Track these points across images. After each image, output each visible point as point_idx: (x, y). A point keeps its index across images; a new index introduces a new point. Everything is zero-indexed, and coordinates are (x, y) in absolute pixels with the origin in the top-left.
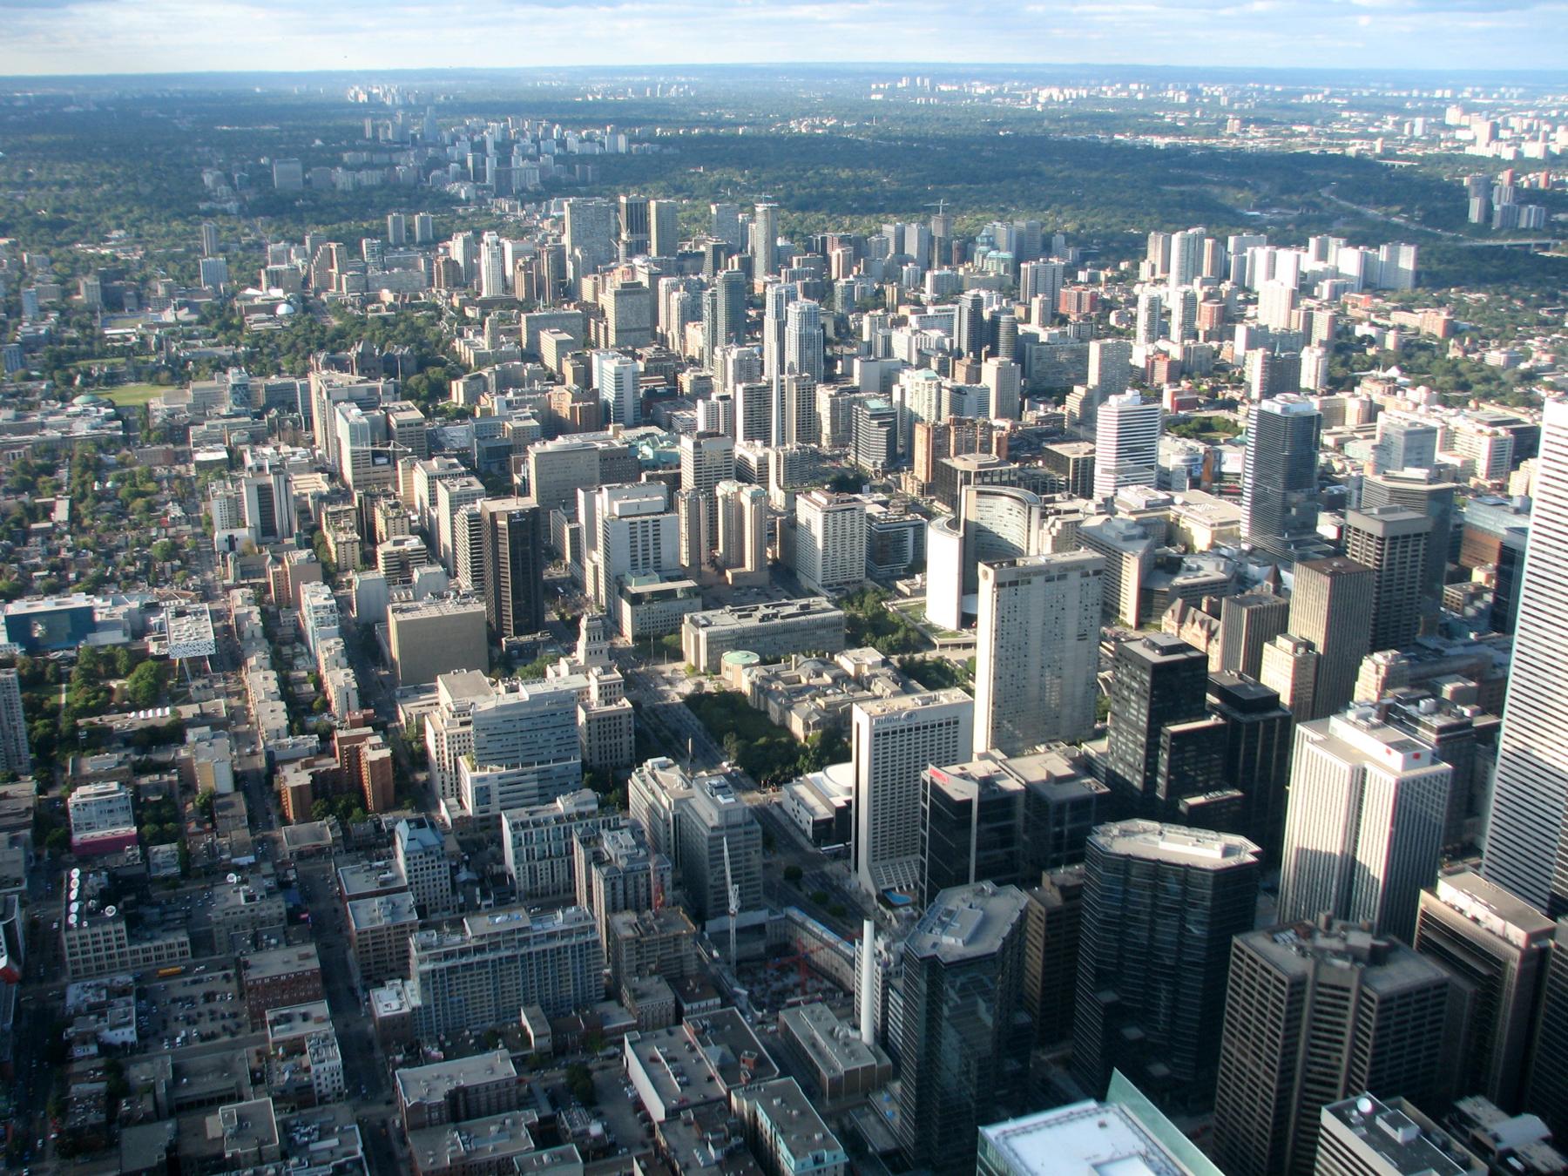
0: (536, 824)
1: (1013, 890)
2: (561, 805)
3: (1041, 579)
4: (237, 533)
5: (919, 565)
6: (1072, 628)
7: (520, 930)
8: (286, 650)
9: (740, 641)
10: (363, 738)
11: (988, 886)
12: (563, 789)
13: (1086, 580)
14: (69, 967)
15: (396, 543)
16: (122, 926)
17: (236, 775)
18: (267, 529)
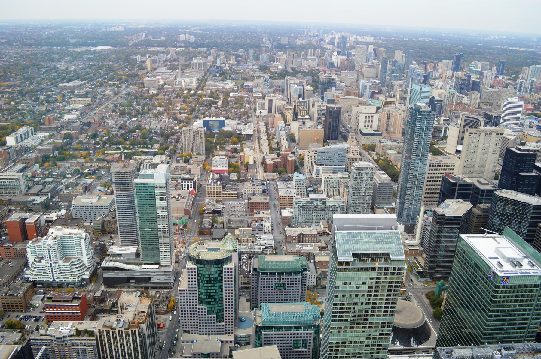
0: (332, 178)
1: (468, 203)
2: (339, 175)
3: (484, 133)
4: (262, 111)
5: (445, 138)
6: (491, 149)
7: (324, 199)
8: (271, 137)
9: (391, 148)
10: (288, 154)
11: (461, 201)
12: (340, 170)
13: (497, 136)
14: (207, 195)
15: (302, 116)
16: (221, 187)
17: (254, 161)
18: (270, 111)
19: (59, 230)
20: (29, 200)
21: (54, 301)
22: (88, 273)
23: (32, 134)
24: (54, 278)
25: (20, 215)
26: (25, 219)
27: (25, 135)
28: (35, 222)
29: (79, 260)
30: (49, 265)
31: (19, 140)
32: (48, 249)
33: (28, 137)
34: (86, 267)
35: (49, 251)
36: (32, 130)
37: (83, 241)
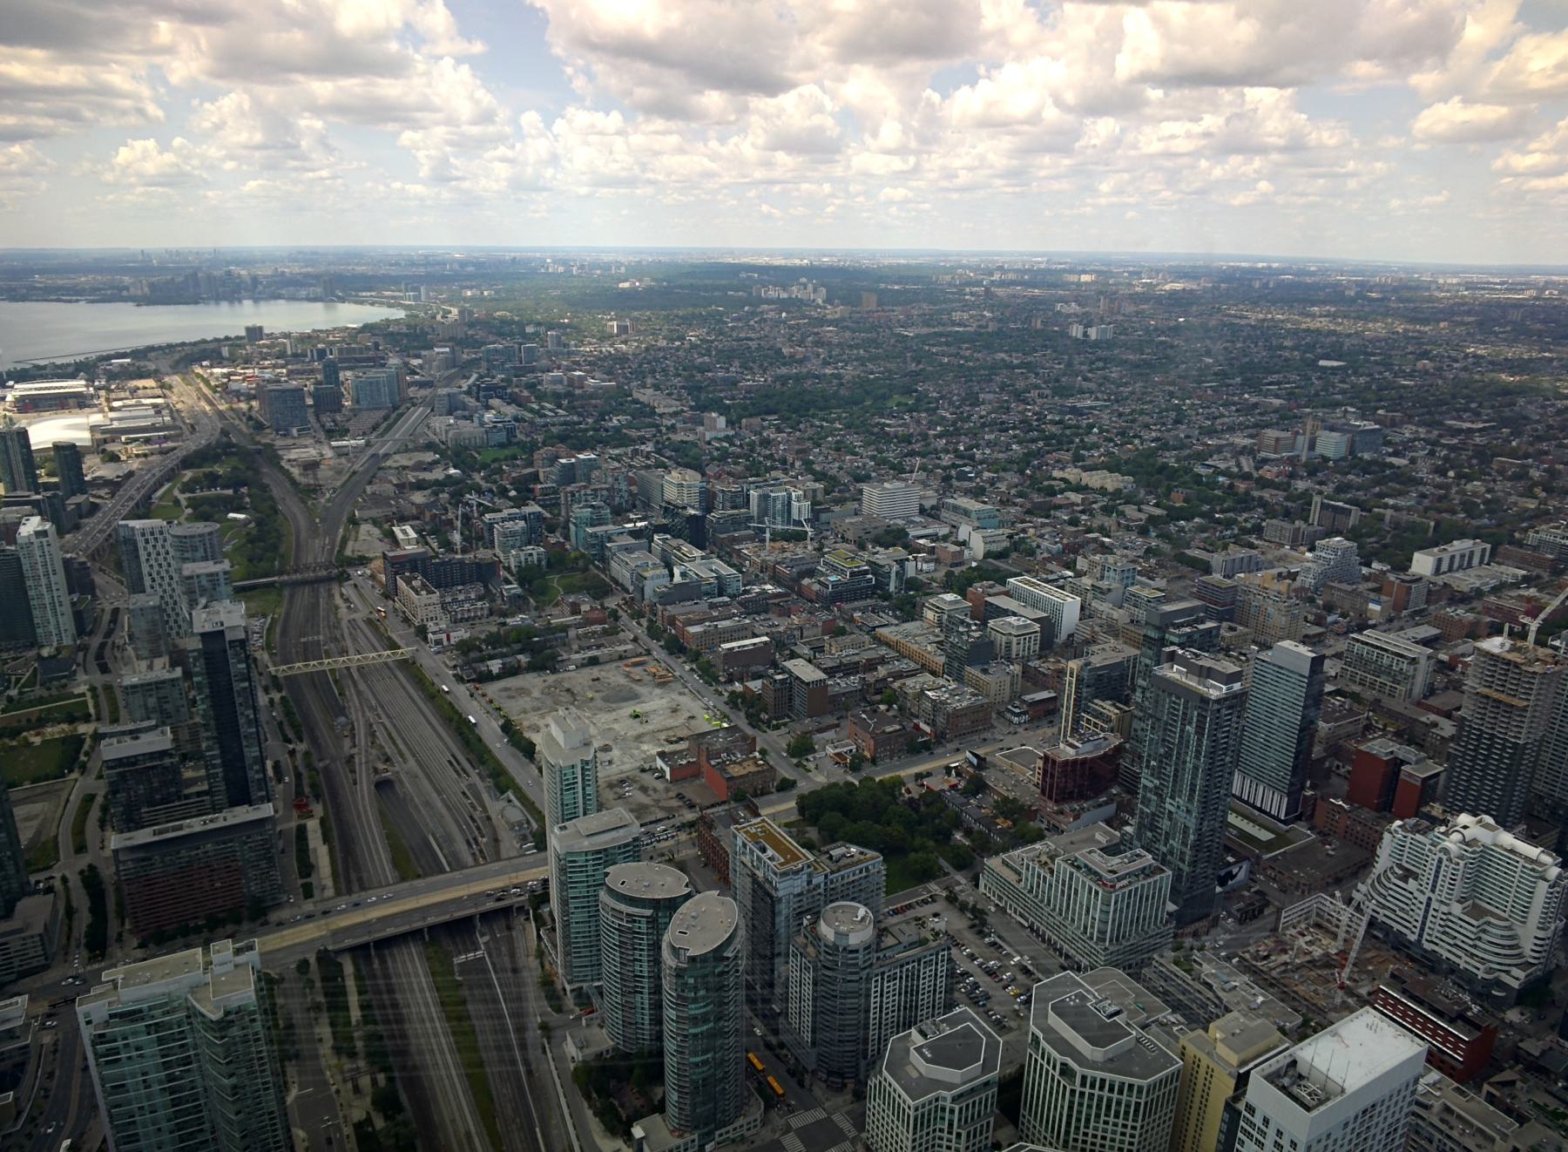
19: (1486, 826)
20: (1423, 719)
21: (1404, 992)
22: (1521, 974)
23: (1481, 562)
24: (1421, 935)
25: (1395, 747)
26: (1403, 762)
27: (1463, 556)
28: (1425, 780)
29: (1509, 928)
30: (1424, 899)
31: (1445, 567)
32: (1440, 861)
33: (1470, 566)
34: (1520, 956)
35: (1439, 867)
36: (1484, 550)
37: (1543, 887)
